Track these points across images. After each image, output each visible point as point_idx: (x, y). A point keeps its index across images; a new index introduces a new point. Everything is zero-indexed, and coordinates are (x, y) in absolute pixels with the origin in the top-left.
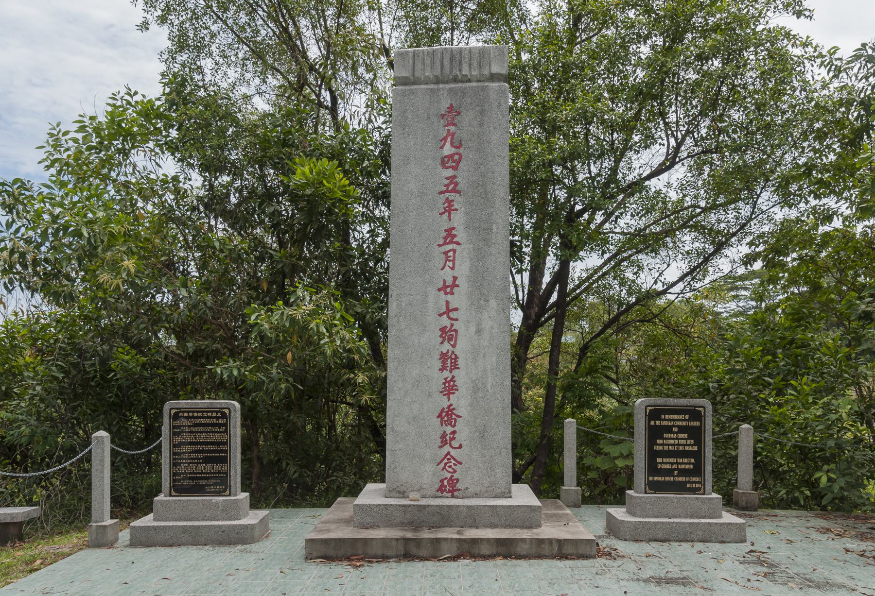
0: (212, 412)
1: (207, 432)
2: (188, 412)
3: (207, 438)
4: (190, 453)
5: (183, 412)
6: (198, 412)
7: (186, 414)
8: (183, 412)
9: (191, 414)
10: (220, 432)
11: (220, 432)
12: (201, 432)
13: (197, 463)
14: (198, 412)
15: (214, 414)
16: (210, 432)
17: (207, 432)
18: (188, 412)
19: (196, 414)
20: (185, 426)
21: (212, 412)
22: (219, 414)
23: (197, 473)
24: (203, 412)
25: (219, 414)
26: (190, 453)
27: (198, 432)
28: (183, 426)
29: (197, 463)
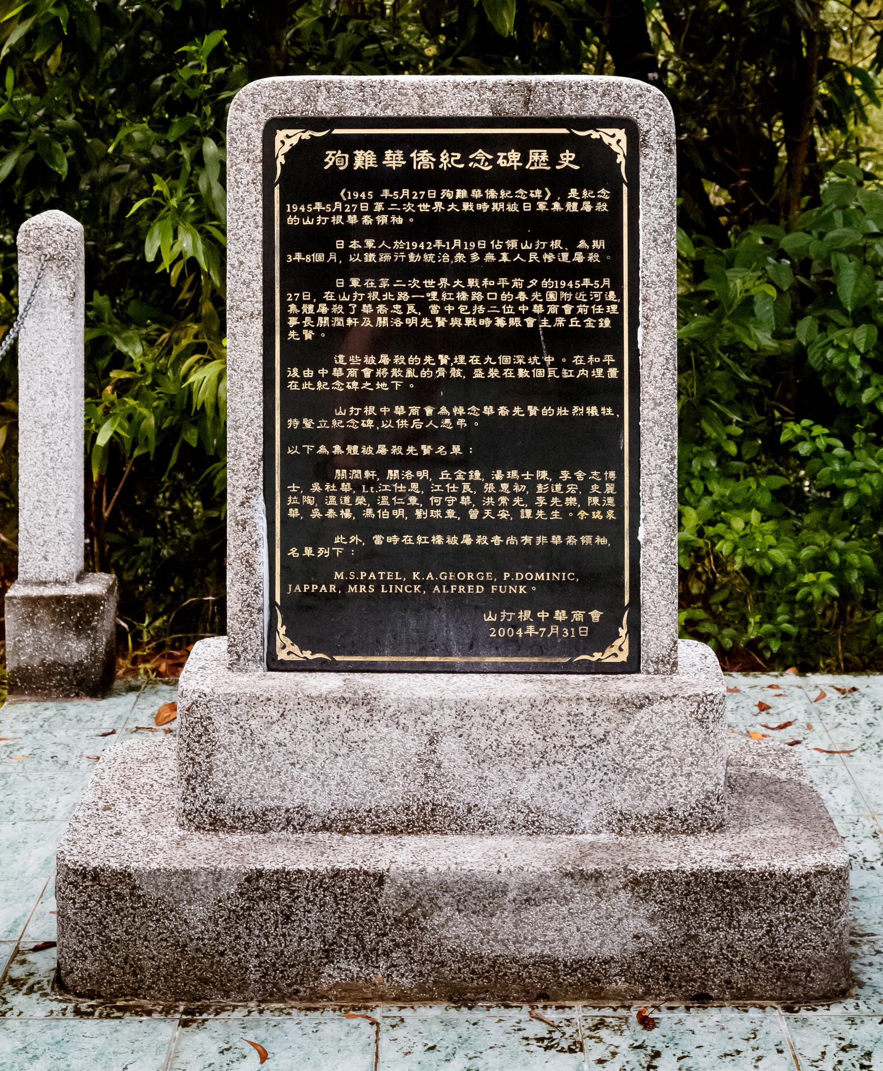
0: (524, 145)
1: (495, 270)
2: (379, 145)
3: (493, 307)
4: (392, 398)
5: (349, 145)
6: (435, 145)
7: (364, 159)
8: (349, 145)
9: (393, 159)
10: (573, 271)
11: (573, 271)
12: (464, 271)
13: (434, 463)
14: (435, 145)
15: (539, 158)
16: (510, 270)
17: (495, 270)
18: (379, 145)
19: (423, 159)
20: (360, 232)
21: (524, 145)
22: (567, 158)
23: (429, 527)
24: (465, 145)
25: (567, 158)
26: (392, 398)
27: (436, 271)
28: (347, 232)
29: (434, 463)
